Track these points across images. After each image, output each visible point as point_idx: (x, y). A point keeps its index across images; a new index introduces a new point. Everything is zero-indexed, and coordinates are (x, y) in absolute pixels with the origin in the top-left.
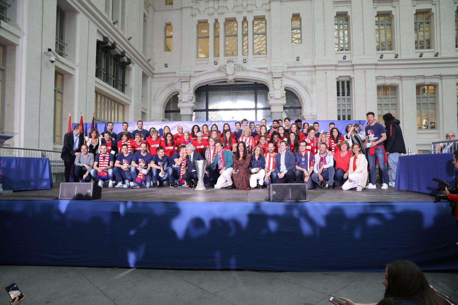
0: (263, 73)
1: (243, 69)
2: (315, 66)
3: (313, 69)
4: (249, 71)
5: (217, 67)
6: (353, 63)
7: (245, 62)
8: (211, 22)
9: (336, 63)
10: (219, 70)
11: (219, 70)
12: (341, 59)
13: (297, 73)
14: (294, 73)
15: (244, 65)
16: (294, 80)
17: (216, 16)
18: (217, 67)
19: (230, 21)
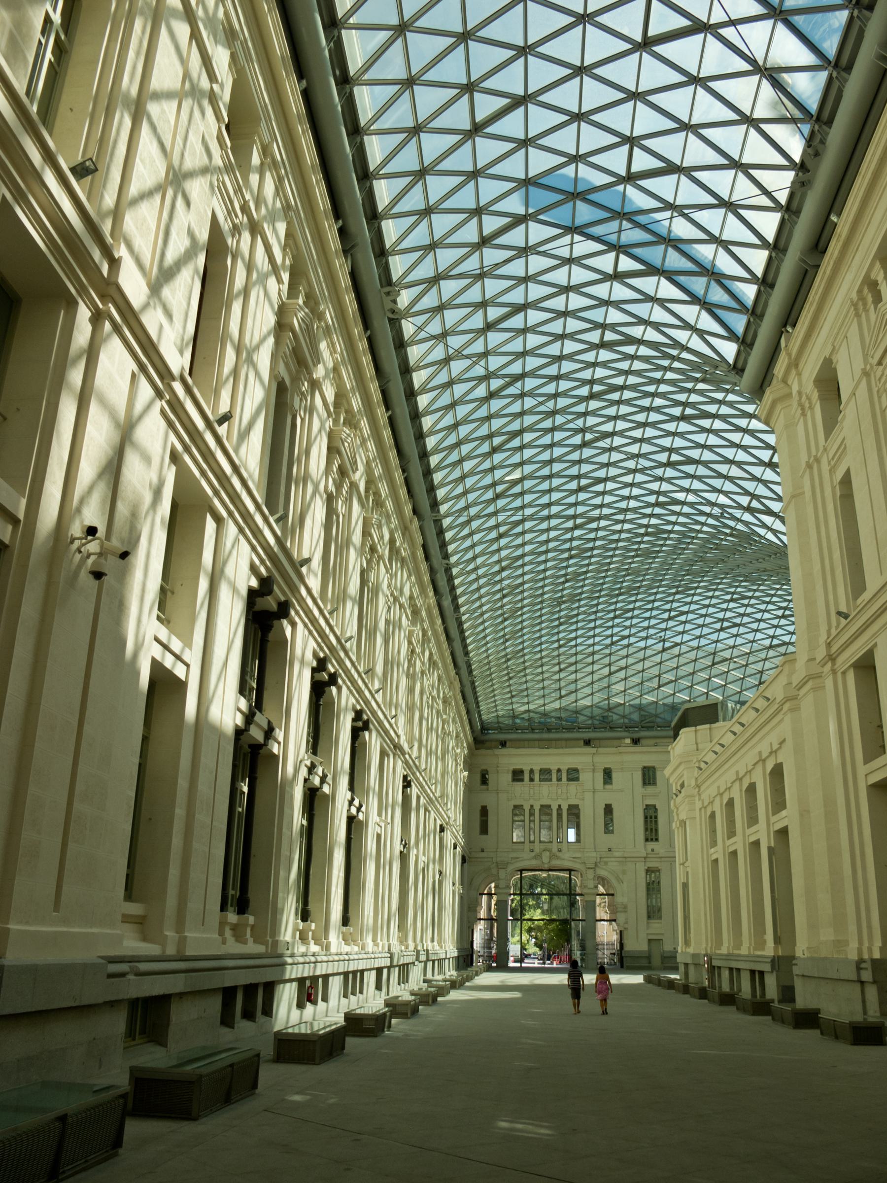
0: (576, 862)
1: (558, 858)
2: (625, 858)
3: (624, 859)
4: (563, 859)
5: (533, 854)
6: (660, 856)
7: (560, 850)
8: (527, 808)
9: (645, 855)
10: (535, 857)
11: (535, 857)
12: (649, 850)
13: (609, 863)
14: (606, 863)
15: (558, 854)
16: (606, 870)
17: (531, 802)
18: (533, 854)
19: (545, 809)
